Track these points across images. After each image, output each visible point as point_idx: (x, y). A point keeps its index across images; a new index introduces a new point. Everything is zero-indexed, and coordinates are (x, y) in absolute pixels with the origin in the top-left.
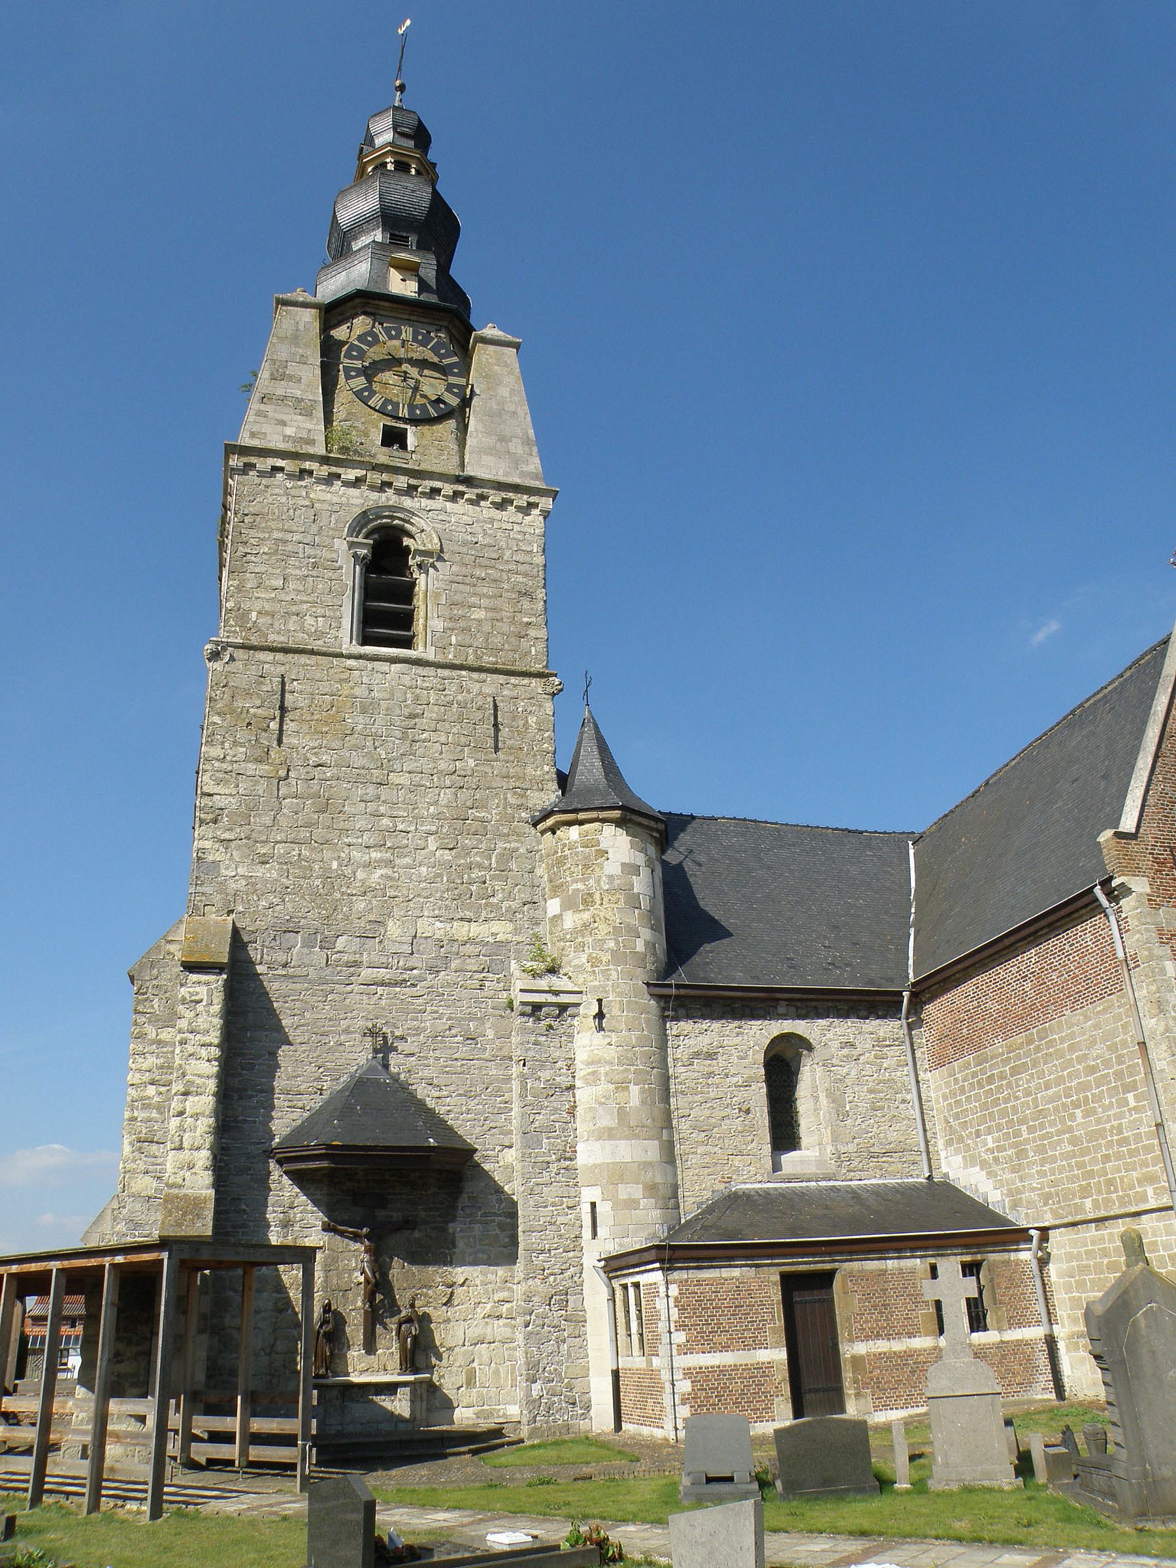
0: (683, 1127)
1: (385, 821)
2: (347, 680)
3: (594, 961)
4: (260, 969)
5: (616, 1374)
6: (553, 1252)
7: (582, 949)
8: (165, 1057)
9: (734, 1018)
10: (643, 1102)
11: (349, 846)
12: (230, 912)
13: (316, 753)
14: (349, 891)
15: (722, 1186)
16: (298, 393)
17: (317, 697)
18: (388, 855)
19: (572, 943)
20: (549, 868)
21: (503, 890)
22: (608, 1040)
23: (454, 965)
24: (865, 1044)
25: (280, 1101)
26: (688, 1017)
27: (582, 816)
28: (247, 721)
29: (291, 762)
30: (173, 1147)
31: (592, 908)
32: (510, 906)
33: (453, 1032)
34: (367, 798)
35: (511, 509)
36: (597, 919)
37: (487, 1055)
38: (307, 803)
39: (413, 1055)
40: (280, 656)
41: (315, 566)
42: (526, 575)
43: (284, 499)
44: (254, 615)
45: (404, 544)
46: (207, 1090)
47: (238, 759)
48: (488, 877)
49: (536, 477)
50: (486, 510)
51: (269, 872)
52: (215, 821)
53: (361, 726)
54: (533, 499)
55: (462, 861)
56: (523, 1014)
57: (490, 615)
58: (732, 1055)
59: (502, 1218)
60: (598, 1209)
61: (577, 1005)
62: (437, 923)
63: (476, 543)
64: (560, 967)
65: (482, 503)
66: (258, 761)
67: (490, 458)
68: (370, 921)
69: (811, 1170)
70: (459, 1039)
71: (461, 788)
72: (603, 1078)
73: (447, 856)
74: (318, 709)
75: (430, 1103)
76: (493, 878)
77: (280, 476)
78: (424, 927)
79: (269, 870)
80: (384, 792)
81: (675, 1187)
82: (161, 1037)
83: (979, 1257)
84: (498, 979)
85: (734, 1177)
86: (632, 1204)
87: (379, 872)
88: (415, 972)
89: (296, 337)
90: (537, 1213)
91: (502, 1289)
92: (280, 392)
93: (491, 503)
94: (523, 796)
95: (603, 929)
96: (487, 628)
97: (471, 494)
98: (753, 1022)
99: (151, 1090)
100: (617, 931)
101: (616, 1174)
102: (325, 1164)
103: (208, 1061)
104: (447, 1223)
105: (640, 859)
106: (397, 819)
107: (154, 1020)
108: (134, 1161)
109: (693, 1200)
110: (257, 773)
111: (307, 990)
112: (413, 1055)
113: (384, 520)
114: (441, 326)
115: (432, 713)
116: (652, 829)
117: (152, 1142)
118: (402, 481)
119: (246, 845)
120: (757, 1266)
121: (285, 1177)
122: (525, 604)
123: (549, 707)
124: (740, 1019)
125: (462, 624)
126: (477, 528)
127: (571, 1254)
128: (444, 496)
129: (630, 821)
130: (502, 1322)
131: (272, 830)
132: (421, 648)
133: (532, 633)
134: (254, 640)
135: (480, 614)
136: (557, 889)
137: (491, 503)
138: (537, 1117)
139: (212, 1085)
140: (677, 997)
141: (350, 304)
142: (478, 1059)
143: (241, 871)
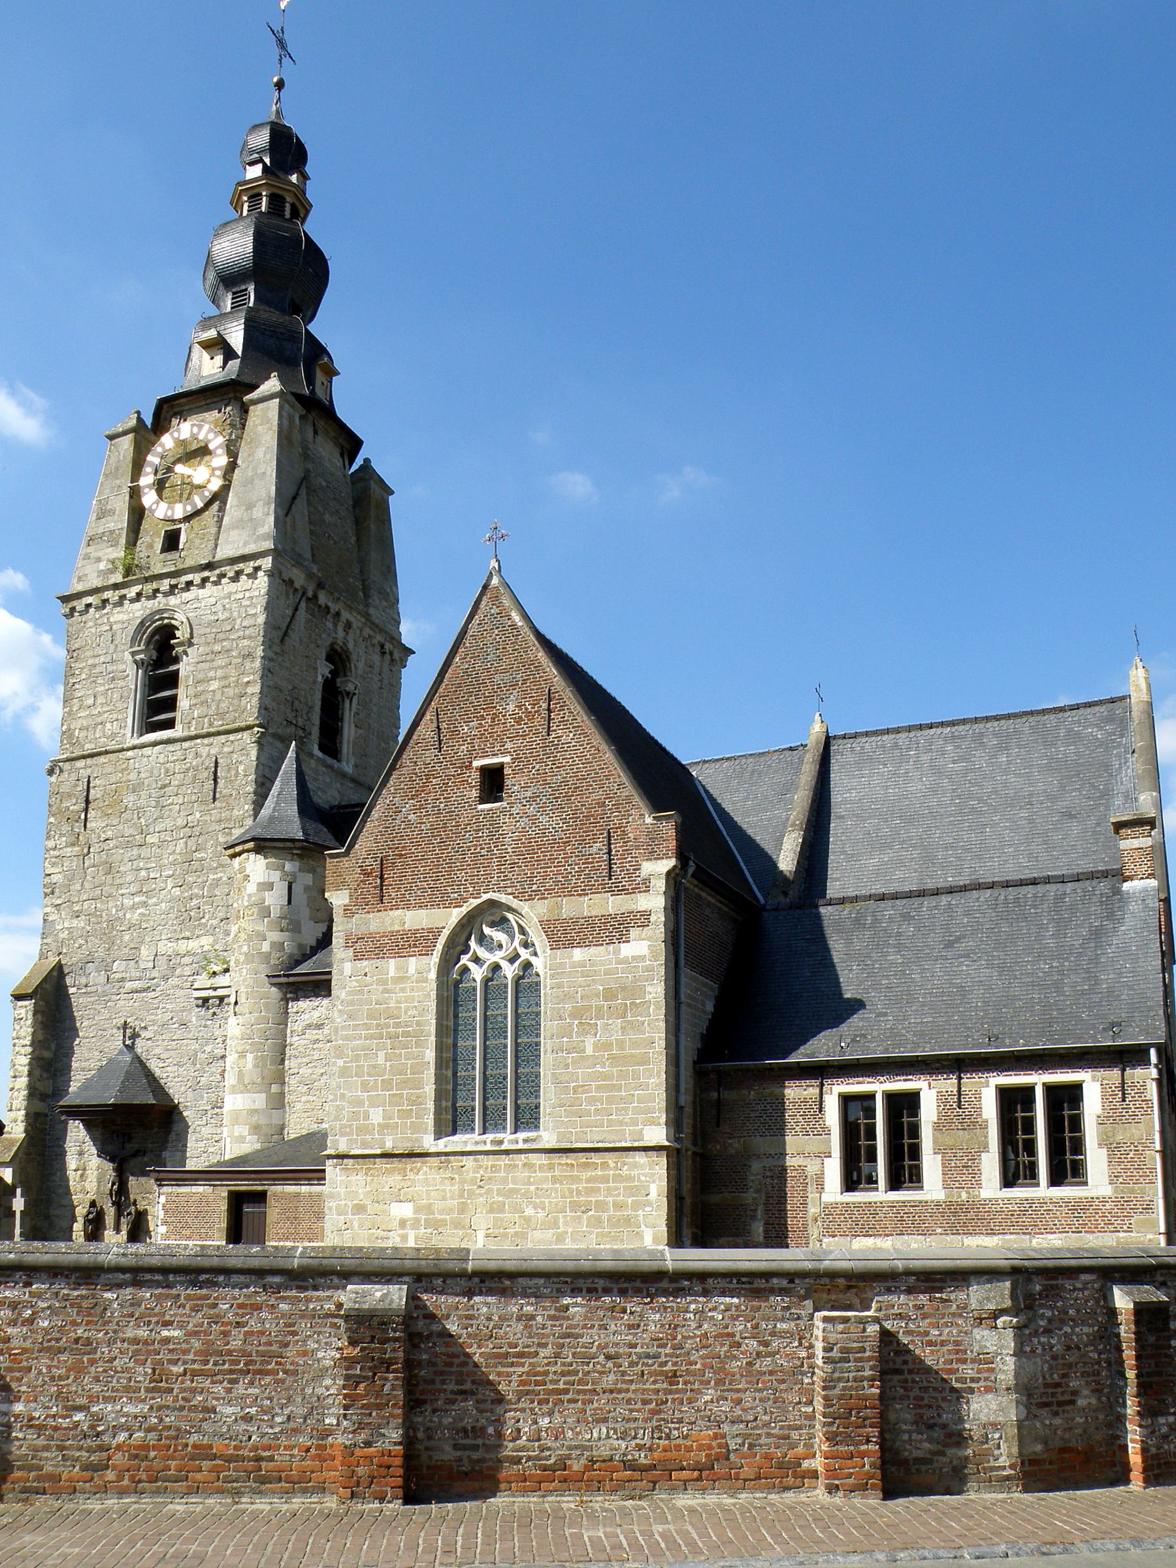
0: (292, 1081)
1: (143, 873)
4: (72, 990)
10: (255, 1066)
12: (60, 953)
15: (316, 1126)
16: (111, 526)
23: (178, 972)
26: (306, 997)
27: (238, 849)
34: (133, 858)
35: (244, 577)
37: (191, 1036)
40: (89, 761)
41: (113, 679)
42: (250, 638)
43: (93, 630)
44: (77, 731)
49: (265, 537)
50: (227, 586)
51: (80, 923)
52: (53, 893)
54: (258, 563)
56: (198, 1006)
61: (229, 996)
65: (224, 581)
66: (73, 845)
70: (176, 1025)
73: (177, 892)
75: (158, 1072)
77: (92, 610)
78: (163, 947)
80: (145, 852)
81: (282, 1127)
87: (139, 911)
89: (117, 469)
92: (101, 531)
95: (243, 936)
96: (218, 696)
100: (250, 938)
105: (275, 876)
113: (158, 623)
114: (230, 399)
116: (291, 848)
118: (165, 585)
119: (68, 906)
122: (248, 665)
125: (203, 698)
126: (219, 607)
128: (196, 586)
129: (265, 847)
133: (250, 690)
137: (229, 578)
138: (202, 1079)
140: (288, 984)
141: (164, 411)
143: (66, 925)
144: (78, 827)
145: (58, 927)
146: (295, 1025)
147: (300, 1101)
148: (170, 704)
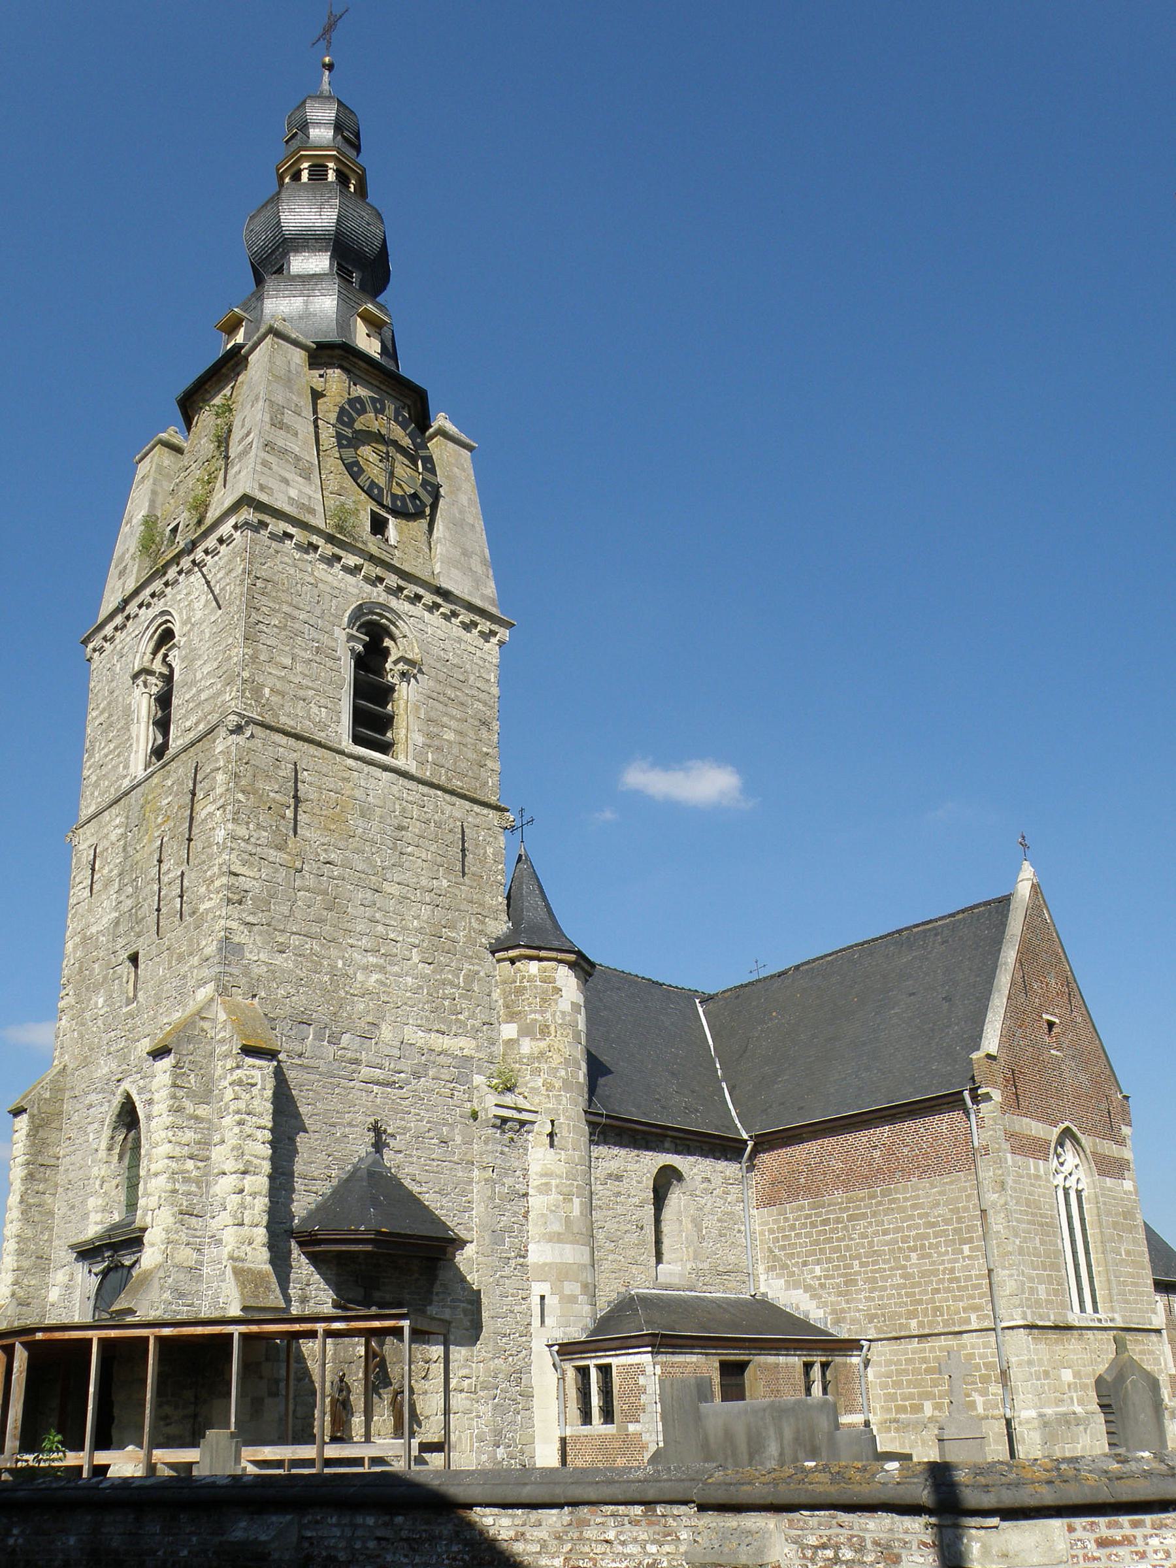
2: (347, 780)
3: (549, 1087)
5: (563, 1441)
6: (512, 1336)
7: (538, 1073)
8: (202, 1133)
9: (635, 1148)
10: (581, 1213)
11: (352, 947)
13: (325, 850)
14: (351, 992)
17: (324, 792)
18: (382, 961)
19: (529, 1067)
20: (505, 995)
21: (469, 1009)
22: (558, 1157)
24: (717, 1180)
25: (299, 1184)
26: (606, 1143)
27: (543, 954)
28: (269, 805)
29: (305, 855)
30: (236, 1223)
31: (547, 1039)
32: (474, 1025)
33: (431, 1134)
36: (552, 1049)
37: (456, 1158)
38: (318, 898)
39: (400, 1152)
40: (292, 741)
42: (485, 704)
45: (385, 644)
46: (263, 1171)
47: (261, 843)
48: (457, 995)
50: (454, 629)
53: (361, 830)
54: (495, 627)
55: (439, 977)
56: (494, 1126)
57: (458, 738)
58: (632, 1179)
59: (464, 1305)
60: (546, 1301)
61: (533, 1123)
62: (419, 1032)
63: (447, 661)
64: (515, 1086)
66: (279, 848)
67: (457, 572)
68: (369, 1023)
69: (676, 1281)
70: (435, 1141)
71: (438, 906)
72: (554, 1190)
73: (428, 969)
74: (326, 804)
76: (461, 996)
79: (286, 960)
82: (199, 1112)
83: (830, 1359)
84: (464, 1090)
85: (631, 1282)
86: (572, 1299)
87: (375, 977)
88: (402, 1075)
90: (501, 1302)
91: (465, 1366)
93: (460, 622)
94: (483, 923)
95: (557, 1060)
97: (446, 608)
98: (646, 1153)
99: (190, 1165)
101: (560, 1274)
102: (369, 1248)
103: (263, 1143)
104: (426, 1306)
106: (388, 927)
107: (191, 1094)
108: (177, 1232)
109: (604, 1299)
110: (278, 860)
111: (319, 1081)
112: (400, 1152)
113: (375, 617)
115: (415, 828)
117: (192, 1215)
120: (707, 1354)
121: (303, 1256)
122: (484, 734)
123: (502, 839)
124: (638, 1149)
125: (436, 743)
127: (524, 1339)
128: (424, 604)
130: (464, 1395)
131: (288, 920)
132: (402, 757)
134: (269, 719)
135: (449, 736)
136: (512, 1016)
137: (460, 622)
138: (503, 1218)
139: (266, 1167)
142: (450, 1161)
143: (263, 957)
144: (286, 828)
145: (249, 956)
146: (599, 1172)
147: (606, 1259)
148: (386, 722)
